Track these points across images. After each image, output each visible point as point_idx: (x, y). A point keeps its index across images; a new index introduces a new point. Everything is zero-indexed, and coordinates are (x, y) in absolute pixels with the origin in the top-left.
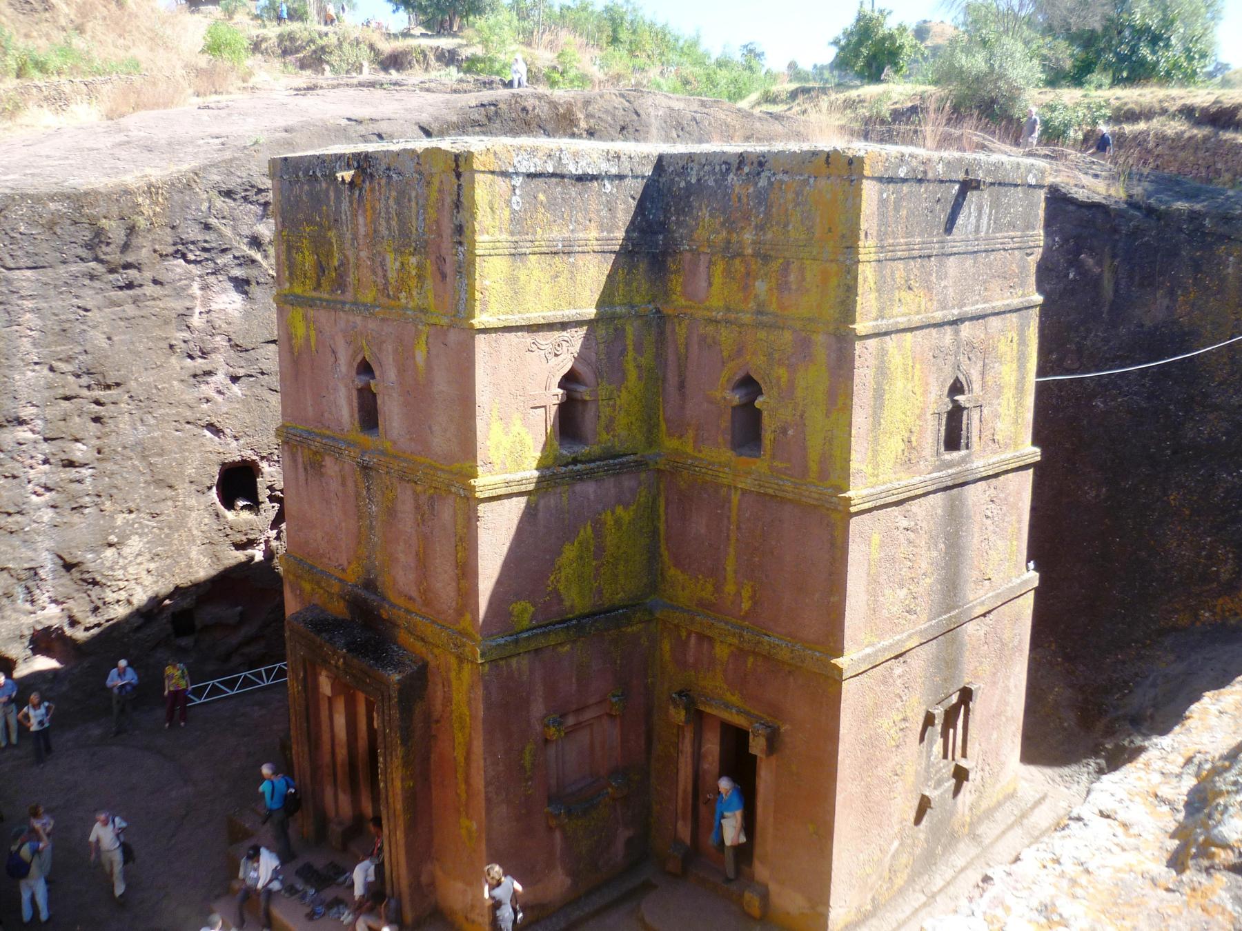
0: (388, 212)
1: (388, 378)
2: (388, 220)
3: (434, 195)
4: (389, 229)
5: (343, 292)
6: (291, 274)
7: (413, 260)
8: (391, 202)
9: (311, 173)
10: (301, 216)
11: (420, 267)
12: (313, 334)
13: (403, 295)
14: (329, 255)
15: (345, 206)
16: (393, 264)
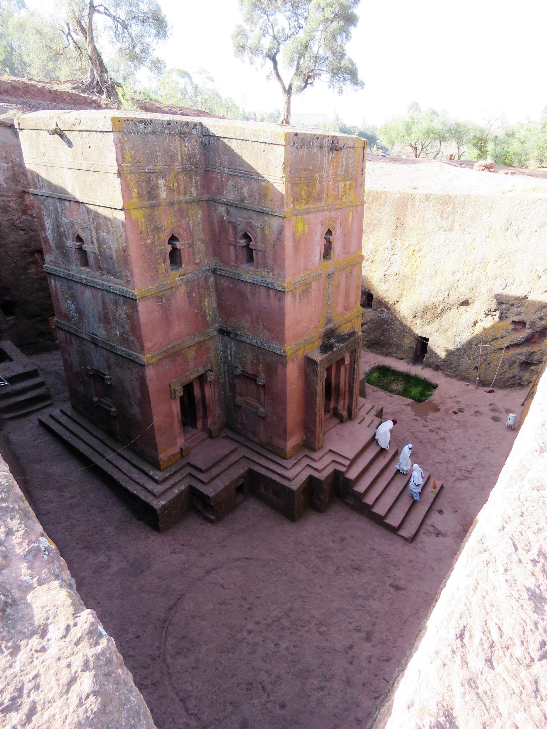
0: (342, 164)
1: (338, 234)
2: (342, 167)
3: (357, 156)
4: (341, 171)
5: (320, 202)
6: (294, 200)
7: (348, 183)
8: (344, 160)
9: (311, 144)
10: (302, 167)
11: (350, 185)
12: (307, 227)
13: (344, 198)
14: (314, 186)
15: (325, 161)
16: (341, 185)
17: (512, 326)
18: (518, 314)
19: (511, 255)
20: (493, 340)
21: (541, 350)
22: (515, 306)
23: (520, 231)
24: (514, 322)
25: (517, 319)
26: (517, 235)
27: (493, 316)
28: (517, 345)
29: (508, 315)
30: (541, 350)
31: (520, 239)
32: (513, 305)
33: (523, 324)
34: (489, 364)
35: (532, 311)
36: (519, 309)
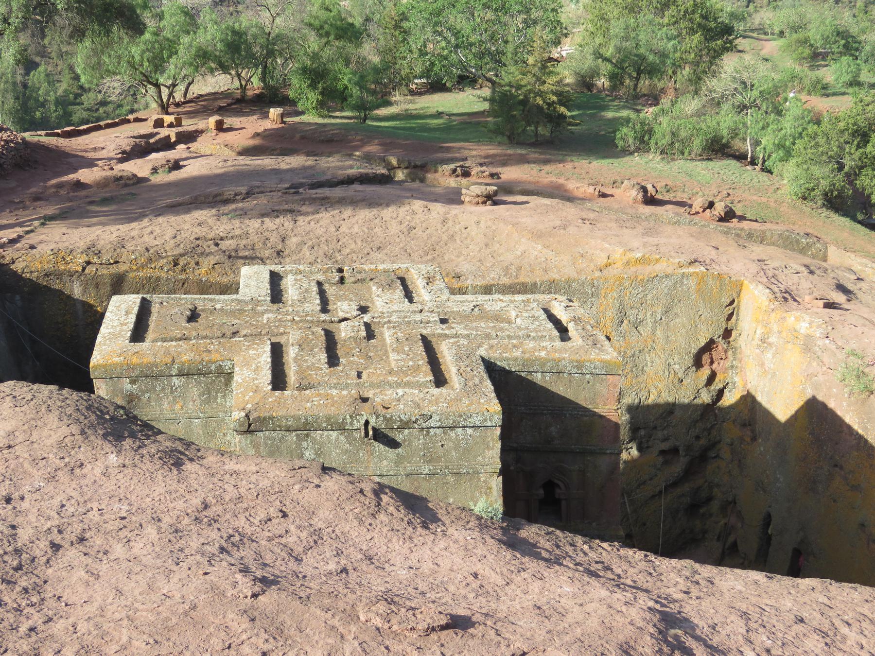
17: (661, 459)
18: (665, 440)
19: (636, 357)
20: (639, 486)
21: (705, 482)
22: (659, 429)
23: (640, 322)
24: (662, 452)
25: (665, 446)
26: (636, 328)
27: (627, 450)
28: (675, 484)
29: (650, 443)
30: (706, 482)
31: (642, 332)
32: (655, 428)
33: (675, 451)
34: (644, 524)
35: (684, 431)
36: (665, 432)
